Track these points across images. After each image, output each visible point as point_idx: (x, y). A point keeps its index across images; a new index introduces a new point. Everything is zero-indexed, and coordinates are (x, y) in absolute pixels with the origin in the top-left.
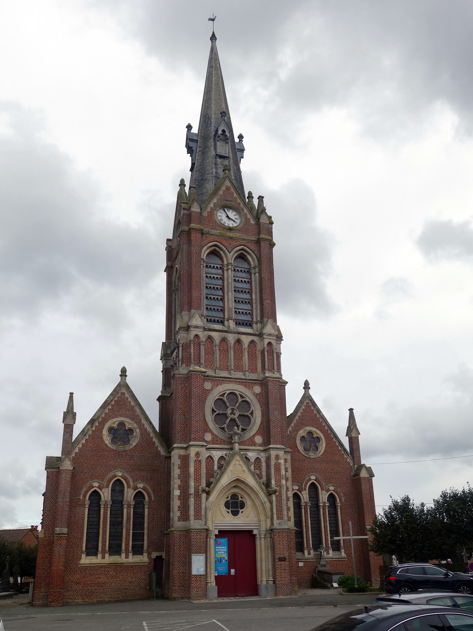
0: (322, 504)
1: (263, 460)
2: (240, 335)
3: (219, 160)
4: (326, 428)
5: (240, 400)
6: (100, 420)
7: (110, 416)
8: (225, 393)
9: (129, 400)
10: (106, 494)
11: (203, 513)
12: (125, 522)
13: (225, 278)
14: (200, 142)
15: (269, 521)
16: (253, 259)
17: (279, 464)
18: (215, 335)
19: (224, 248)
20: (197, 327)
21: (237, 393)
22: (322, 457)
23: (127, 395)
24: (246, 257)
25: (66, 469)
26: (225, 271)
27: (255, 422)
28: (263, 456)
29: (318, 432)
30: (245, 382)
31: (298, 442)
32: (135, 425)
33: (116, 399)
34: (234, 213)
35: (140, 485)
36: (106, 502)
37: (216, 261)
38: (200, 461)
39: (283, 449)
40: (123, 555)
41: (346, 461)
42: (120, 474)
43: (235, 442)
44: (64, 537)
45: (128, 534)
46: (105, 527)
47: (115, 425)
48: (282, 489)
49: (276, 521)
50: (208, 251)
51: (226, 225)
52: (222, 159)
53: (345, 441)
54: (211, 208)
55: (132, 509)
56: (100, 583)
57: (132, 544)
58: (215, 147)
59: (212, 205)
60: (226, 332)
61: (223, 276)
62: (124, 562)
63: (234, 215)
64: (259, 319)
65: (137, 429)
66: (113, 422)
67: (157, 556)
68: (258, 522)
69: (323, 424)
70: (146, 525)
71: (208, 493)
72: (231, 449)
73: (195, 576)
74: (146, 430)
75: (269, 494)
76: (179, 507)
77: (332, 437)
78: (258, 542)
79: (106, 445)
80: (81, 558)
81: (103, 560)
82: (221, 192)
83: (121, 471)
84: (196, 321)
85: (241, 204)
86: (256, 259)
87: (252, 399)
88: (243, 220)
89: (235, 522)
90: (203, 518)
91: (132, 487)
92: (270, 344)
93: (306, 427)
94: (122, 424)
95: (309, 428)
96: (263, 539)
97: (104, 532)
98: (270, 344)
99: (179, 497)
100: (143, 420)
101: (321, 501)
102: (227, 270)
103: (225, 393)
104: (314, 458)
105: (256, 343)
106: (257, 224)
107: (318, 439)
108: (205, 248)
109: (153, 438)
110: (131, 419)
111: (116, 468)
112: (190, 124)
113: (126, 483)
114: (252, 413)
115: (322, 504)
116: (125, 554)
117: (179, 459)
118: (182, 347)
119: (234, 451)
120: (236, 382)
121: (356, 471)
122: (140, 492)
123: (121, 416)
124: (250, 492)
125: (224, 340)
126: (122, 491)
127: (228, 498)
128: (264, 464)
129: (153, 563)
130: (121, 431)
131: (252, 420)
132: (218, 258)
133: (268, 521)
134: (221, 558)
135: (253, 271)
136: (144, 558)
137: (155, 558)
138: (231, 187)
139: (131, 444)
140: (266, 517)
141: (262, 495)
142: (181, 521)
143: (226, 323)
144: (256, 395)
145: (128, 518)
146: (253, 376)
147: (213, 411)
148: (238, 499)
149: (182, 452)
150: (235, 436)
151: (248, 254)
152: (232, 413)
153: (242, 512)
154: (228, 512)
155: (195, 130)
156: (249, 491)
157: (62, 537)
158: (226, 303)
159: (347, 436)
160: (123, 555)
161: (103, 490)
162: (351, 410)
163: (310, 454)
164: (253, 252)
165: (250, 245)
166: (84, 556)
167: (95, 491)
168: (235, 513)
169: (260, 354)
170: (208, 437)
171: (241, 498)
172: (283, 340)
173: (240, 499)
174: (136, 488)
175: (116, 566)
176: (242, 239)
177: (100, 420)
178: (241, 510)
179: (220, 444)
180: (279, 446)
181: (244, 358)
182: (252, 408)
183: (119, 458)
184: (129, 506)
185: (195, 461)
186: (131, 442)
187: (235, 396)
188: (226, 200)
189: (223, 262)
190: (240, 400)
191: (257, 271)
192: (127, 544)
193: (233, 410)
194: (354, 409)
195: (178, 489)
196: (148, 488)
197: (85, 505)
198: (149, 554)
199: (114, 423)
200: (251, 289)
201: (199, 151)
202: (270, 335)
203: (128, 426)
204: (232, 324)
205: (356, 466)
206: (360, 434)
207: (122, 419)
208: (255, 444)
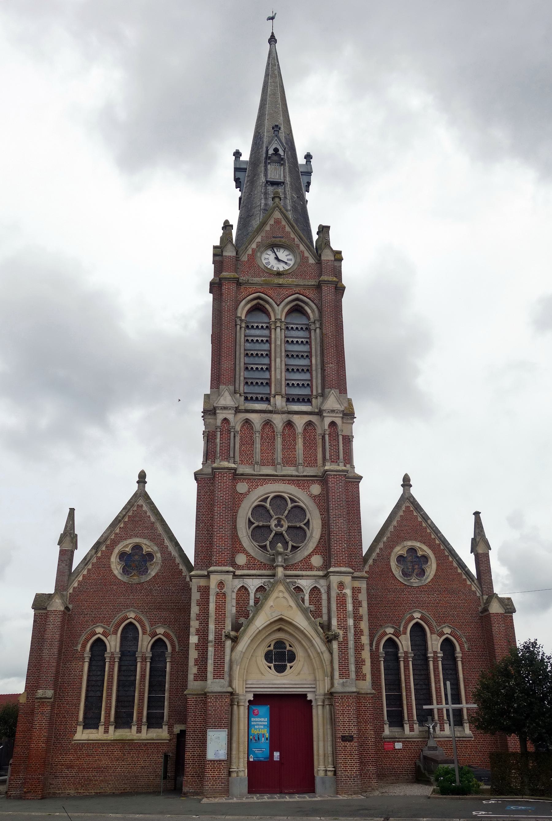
0: (432, 655)
2: (291, 416)
3: (270, 188)
4: (437, 542)
5: (290, 505)
6: (108, 542)
7: (121, 537)
8: (267, 498)
9: (148, 514)
10: (113, 643)
11: (226, 668)
12: (137, 682)
13: (273, 340)
15: (327, 680)
16: (313, 311)
17: (345, 595)
18: (253, 417)
19: (271, 300)
20: (225, 408)
21: (286, 495)
22: (430, 584)
23: (145, 508)
25: (55, 609)
26: (273, 331)
27: (311, 536)
28: (322, 585)
29: (425, 548)
30: (298, 480)
31: (393, 563)
32: (156, 548)
33: (130, 514)
34: (286, 253)
35: (160, 631)
36: (112, 654)
37: (260, 319)
38: (224, 593)
39: (349, 573)
40: (134, 728)
41: (470, 589)
42: (132, 615)
43: (277, 566)
44: (48, 702)
45: (141, 699)
46: (110, 688)
47: (128, 549)
48: (348, 632)
49: (337, 680)
50: (249, 306)
52: (275, 186)
54: (253, 249)
55: (148, 664)
56: (100, 768)
58: (266, 173)
59: (254, 246)
60: (271, 412)
61: (270, 337)
62: (135, 738)
63: (286, 256)
65: (157, 553)
66: (126, 545)
67: (181, 730)
69: (433, 536)
70: (167, 686)
71: (235, 640)
72: (274, 575)
73: (211, 761)
74: (170, 553)
75: (328, 640)
76: (196, 660)
77: (447, 554)
79: (115, 576)
80: (76, 732)
81: (106, 735)
83: (134, 612)
84: (225, 400)
85: (296, 239)
86: (316, 310)
88: (298, 260)
89: (278, 682)
90: (226, 676)
91: (148, 633)
92: (333, 424)
93: (405, 542)
94: (137, 547)
95: (410, 544)
96: (320, 708)
97: (109, 695)
98: (333, 424)
99: (197, 645)
100: (166, 541)
101: (430, 650)
103: (267, 498)
104: (418, 587)
105: (316, 425)
106: (318, 263)
107: (425, 558)
108: (243, 302)
109: (180, 565)
110: (151, 540)
111: (127, 607)
112: (239, 150)
113: (141, 627)
115: (432, 655)
116: (136, 726)
117: (198, 592)
118: (208, 437)
119: (276, 578)
120: (283, 480)
121: (485, 604)
122: (160, 640)
123: (136, 536)
124: (301, 638)
125: (268, 423)
126: (136, 639)
127: (270, 646)
128: (324, 597)
129: (175, 740)
130: (136, 557)
132: (264, 315)
133: (326, 681)
134: (258, 735)
135: (312, 327)
136: (163, 733)
137: (178, 734)
138: (282, 219)
139: (150, 574)
140: (325, 675)
141: (318, 643)
142: (198, 680)
144: (314, 498)
145: (143, 676)
146: (310, 471)
147: (250, 523)
148: (286, 648)
149: (202, 582)
150: (277, 556)
152: (279, 524)
153: (291, 667)
154: (270, 668)
155: (246, 157)
157: (46, 702)
158: (273, 373)
159: (473, 553)
160: (134, 728)
161: (109, 638)
162: (477, 514)
163: (411, 581)
164: (313, 301)
165: (307, 292)
166: (80, 728)
168: (280, 669)
170: (241, 559)
171: (290, 646)
172: (356, 418)
173: (288, 648)
174: (154, 634)
175: (123, 743)
176: (296, 285)
177: (108, 542)
178: (289, 665)
179: (259, 569)
180: (343, 569)
183: (131, 593)
184: (144, 659)
185: (217, 594)
186: (149, 572)
188: (274, 237)
189: (270, 318)
190: (290, 505)
191: (318, 325)
192: (140, 713)
193: (279, 520)
194: (480, 513)
195: (196, 635)
196: (171, 634)
197: (84, 658)
198: (170, 727)
199: (127, 546)
200: (310, 352)
202: (333, 411)
203: (146, 549)
204: (279, 402)
205: (485, 597)
206: (490, 549)
207: (137, 540)
208: (311, 568)
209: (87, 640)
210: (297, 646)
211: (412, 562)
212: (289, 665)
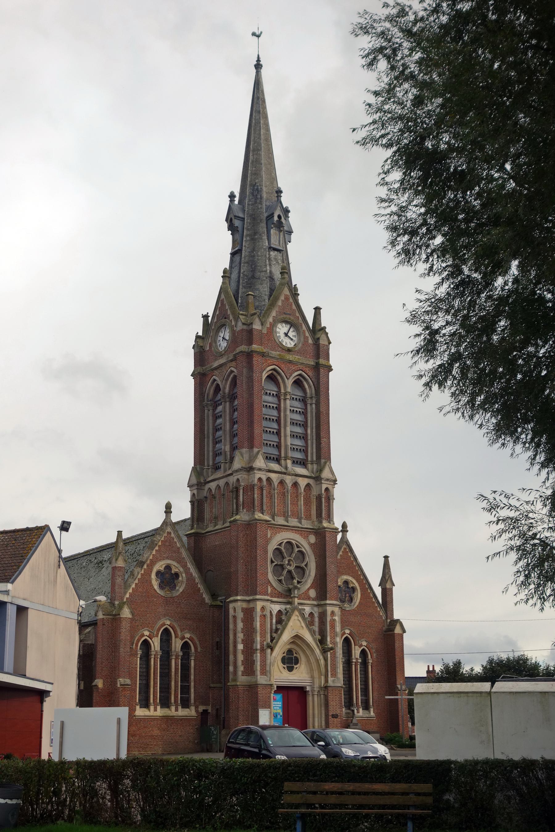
1: (316, 615)
2: (297, 478)
4: (362, 577)
5: (296, 550)
6: (148, 562)
9: (175, 540)
10: (156, 644)
12: (173, 674)
13: (282, 408)
15: (323, 678)
16: (310, 387)
17: (334, 620)
19: (283, 374)
20: (260, 469)
21: (293, 542)
22: (356, 609)
25: (125, 617)
26: (282, 401)
27: (309, 575)
29: (354, 581)
30: (301, 531)
32: (181, 569)
33: (162, 539)
35: (187, 635)
39: (338, 605)
40: (173, 708)
41: (379, 614)
42: (168, 622)
43: (295, 597)
45: (176, 687)
46: (155, 678)
47: (162, 569)
48: (336, 646)
49: (330, 679)
51: (284, 344)
53: (378, 591)
54: (270, 323)
55: (180, 660)
56: (153, 736)
57: (181, 697)
59: (271, 320)
60: (285, 473)
62: (175, 715)
65: (183, 573)
67: (203, 710)
68: (311, 679)
69: (359, 573)
71: (272, 650)
75: (324, 651)
76: (242, 661)
77: (367, 587)
78: (310, 699)
80: (135, 710)
81: (155, 712)
82: (280, 303)
83: (169, 620)
86: (313, 387)
88: (302, 339)
91: (180, 636)
93: (343, 576)
95: (345, 577)
96: (316, 697)
97: (155, 684)
100: (188, 564)
101: (353, 657)
102: (285, 399)
104: (349, 610)
105: (312, 487)
107: (354, 589)
108: (265, 372)
109: (199, 584)
113: (174, 632)
119: (293, 606)
120: (292, 530)
121: (389, 626)
122: (186, 642)
125: (282, 482)
127: (284, 653)
129: (200, 717)
130: (167, 575)
134: (276, 713)
135: (309, 401)
136: (191, 712)
139: (178, 590)
141: (318, 652)
144: (311, 545)
145: (176, 669)
146: (306, 524)
148: (293, 655)
150: (294, 590)
152: (289, 564)
154: (284, 668)
156: (305, 647)
158: (283, 438)
160: (173, 708)
167: (146, 640)
168: (290, 669)
171: (296, 654)
173: (295, 655)
175: (167, 719)
176: (301, 363)
177: (148, 562)
179: (278, 597)
180: (335, 602)
183: (167, 604)
186: (177, 588)
188: (285, 314)
189: (279, 388)
190: (296, 550)
191: (314, 402)
192: (176, 697)
193: (289, 561)
196: (195, 638)
197: (137, 654)
198: (197, 708)
199: (161, 566)
200: (306, 422)
202: (328, 480)
203: (174, 570)
205: (389, 620)
206: (394, 586)
207: (169, 562)
208: (309, 598)
209: (138, 640)
211: (345, 591)
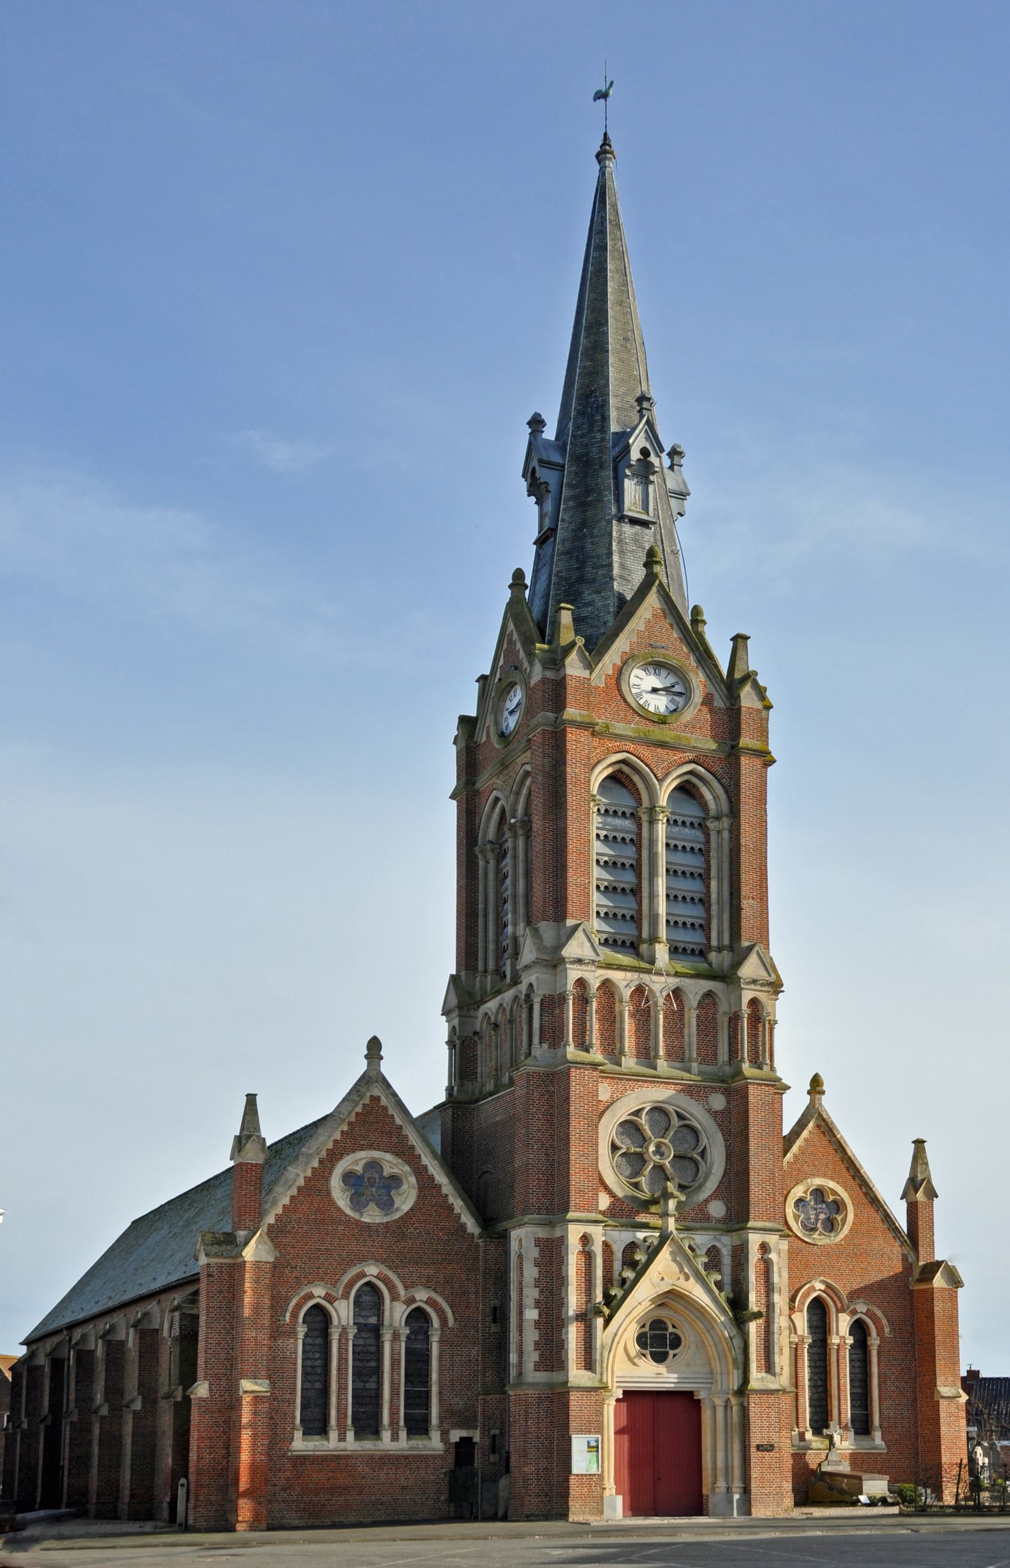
7: (345, 1148)
14: (569, 472)
24: (698, 789)
47: (359, 1168)
64: (726, 941)
66: (355, 1161)
79: (339, 1209)
87: (705, 1123)
114: (703, 1154)
131: (703, 1168)
143: (644, 948)
148: (666, 1329)
151: (703, 783)
153: (674, 1356)
169: (726, 1024)
171: (674, 1327)
173: (671, 1329)
178: (671, 1353)
181: (686, 1031)
182: (704, 1141)
187: (663, 1117)
199: (356, 1162)
201: (567, 499)
210: (686, 1326)
212: (671, 1353)
